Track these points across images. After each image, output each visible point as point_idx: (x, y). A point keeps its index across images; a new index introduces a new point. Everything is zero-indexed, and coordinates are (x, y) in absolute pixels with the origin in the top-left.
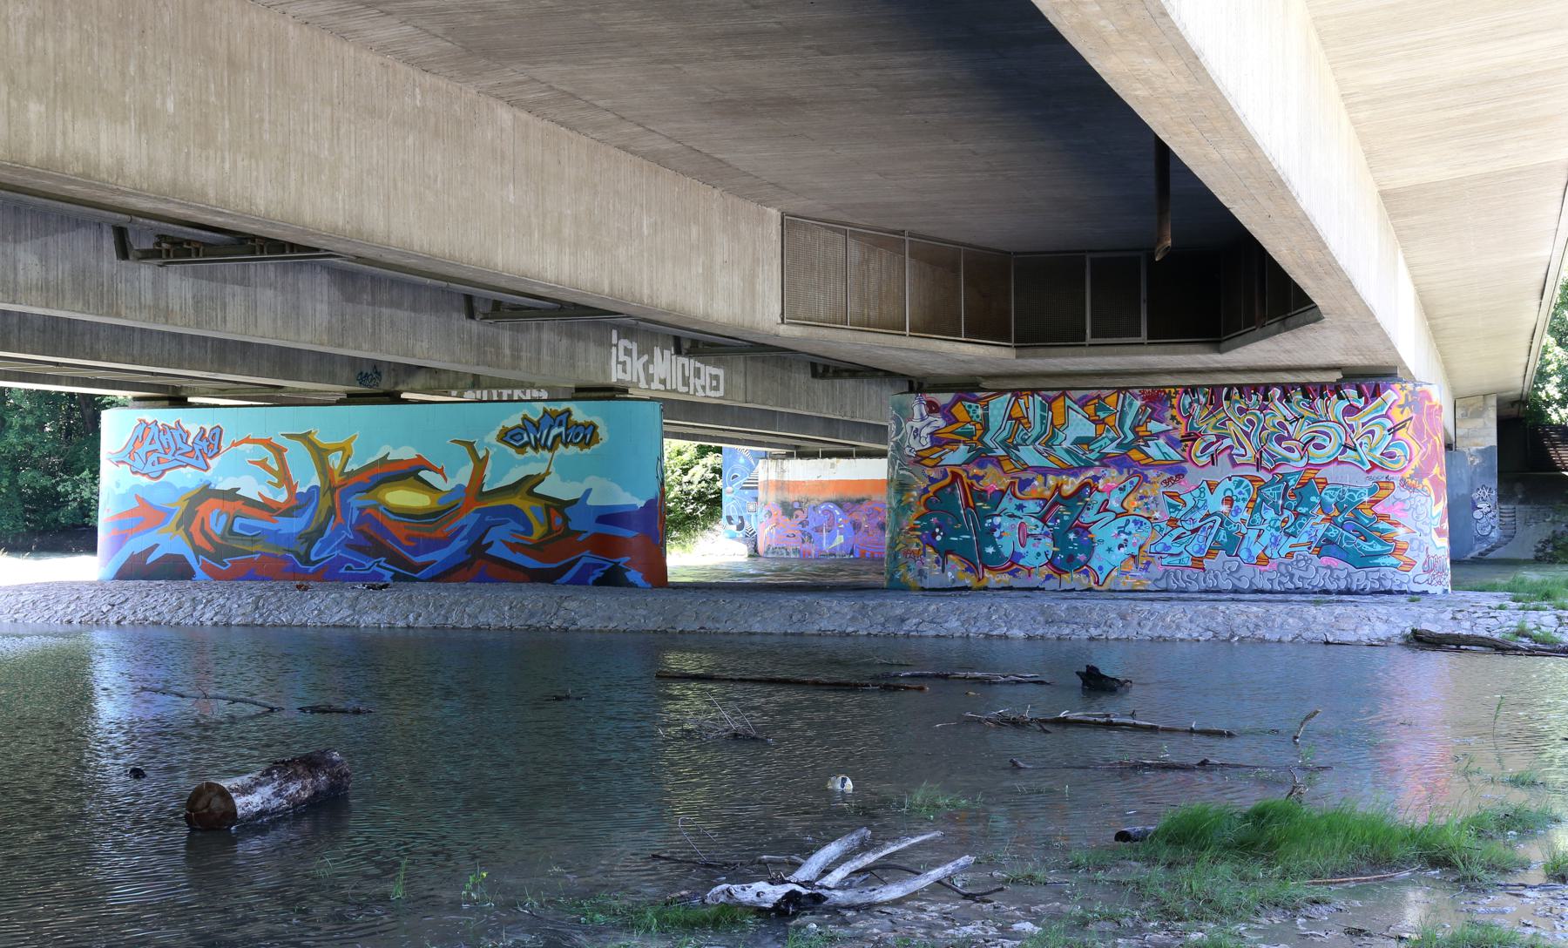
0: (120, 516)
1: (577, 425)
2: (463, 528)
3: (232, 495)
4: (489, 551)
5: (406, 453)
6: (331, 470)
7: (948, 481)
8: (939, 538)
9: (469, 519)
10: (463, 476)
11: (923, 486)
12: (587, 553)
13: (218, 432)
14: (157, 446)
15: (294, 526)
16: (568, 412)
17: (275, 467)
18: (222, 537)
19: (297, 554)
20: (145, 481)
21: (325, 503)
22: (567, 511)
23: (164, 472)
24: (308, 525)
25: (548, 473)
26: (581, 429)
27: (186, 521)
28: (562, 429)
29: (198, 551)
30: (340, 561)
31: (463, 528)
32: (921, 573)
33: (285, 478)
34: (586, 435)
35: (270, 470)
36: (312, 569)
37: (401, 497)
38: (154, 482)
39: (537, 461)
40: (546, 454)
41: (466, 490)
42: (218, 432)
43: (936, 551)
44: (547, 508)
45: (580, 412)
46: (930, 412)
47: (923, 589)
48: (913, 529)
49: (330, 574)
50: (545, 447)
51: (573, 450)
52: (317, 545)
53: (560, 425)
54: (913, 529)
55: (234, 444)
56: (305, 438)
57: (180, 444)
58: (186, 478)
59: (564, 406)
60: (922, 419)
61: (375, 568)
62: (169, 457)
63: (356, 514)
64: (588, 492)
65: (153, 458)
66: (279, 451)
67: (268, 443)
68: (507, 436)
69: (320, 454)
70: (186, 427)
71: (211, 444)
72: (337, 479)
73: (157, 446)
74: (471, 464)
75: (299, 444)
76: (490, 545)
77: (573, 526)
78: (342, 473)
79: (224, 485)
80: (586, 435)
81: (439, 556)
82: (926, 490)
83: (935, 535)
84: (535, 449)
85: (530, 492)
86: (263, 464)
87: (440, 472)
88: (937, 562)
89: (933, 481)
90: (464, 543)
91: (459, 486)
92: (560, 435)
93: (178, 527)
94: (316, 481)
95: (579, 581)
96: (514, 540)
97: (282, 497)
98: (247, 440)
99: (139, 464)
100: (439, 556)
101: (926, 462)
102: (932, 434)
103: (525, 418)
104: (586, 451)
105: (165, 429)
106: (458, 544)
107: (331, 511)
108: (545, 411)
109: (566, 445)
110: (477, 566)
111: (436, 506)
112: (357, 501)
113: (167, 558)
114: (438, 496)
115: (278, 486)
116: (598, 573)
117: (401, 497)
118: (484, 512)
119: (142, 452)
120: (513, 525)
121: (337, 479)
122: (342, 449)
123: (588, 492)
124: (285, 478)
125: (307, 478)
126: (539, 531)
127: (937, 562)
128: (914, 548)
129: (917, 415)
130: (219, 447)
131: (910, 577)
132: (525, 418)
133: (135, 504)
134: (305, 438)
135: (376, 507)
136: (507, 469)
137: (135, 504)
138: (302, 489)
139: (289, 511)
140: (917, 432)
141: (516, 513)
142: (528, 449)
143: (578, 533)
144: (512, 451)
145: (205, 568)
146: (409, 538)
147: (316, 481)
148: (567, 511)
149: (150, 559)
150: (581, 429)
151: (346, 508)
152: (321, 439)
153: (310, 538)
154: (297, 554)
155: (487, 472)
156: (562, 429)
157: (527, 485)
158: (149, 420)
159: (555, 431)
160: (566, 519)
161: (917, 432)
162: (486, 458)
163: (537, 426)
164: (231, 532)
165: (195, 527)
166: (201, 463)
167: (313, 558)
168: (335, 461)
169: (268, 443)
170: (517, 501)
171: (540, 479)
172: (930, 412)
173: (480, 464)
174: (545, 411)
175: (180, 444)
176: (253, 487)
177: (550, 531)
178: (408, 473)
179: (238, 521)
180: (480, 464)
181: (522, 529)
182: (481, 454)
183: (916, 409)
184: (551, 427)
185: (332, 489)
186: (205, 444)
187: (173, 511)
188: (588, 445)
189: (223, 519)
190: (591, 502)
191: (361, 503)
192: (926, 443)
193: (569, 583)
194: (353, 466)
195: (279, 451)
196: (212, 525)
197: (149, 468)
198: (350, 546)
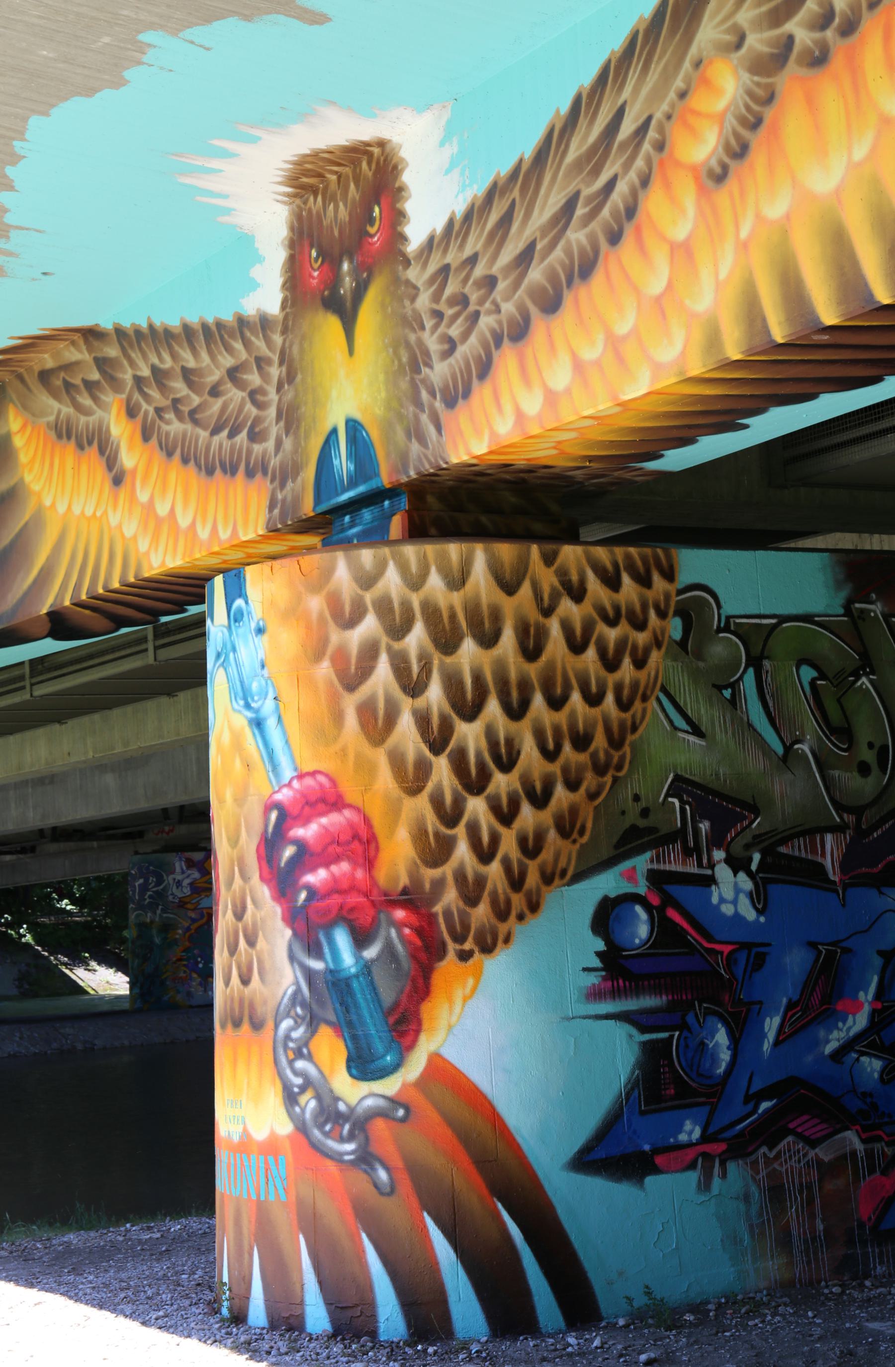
7: (205, 920)
8: (201, 966)
11: (186, 924)
32: (189, 994)
43: (199, 975)
46: (189, 867)
47: (191, 1007)
48: (180, 960)
54: (180, 960)
60: (183, 872)
82: (188, 929)
83: (197, 963)
88: (200, 984)
89: (194, 921)
101: (189, 906)
102: (191, 884)
127: (200, 984)
128: (182, 975)
129: (178, 869)
131: (179, 998)
140: (179, 884)
161: (179, 884)
172: (189, 867)
183: (177, 865)
192: (187, 891)
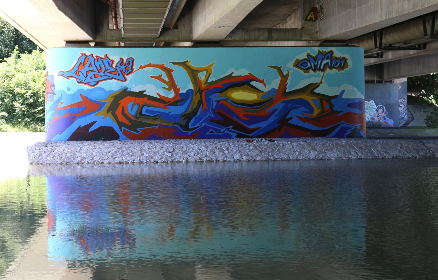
0: (71, 106)
1: (336, 59)
2: (275, 110)
3: (141, 94)
4: (290, 122)
5: (243, 72)
6: (200, 82)
9: (279, 106)
10: (275, 84)
12: (343, 122)
13: (131, 61)
14: (93, 68)
15: (178, 110)
16: (332, 52)
17: (167, 79)
18: (136, 117)
19: (181, 125)
20: (86, 87)
21: (197, 98)
22: (332, 101)
23: (98, 82)
24: (187, 110)
25: (321, 82)
26: (338, 61)
27: (113, 109)
28: (329, 61)
29: (121, 125)
30: (206, 129)
31: (275, 110)
33: (172, 85)
34: (342, 64)
35: (164, 81)
36: (190, 133)
37: (240, 95)
38: (91, 88)
39: (315, 76)
40: (321, 73)
41: (277, 91)
42: (131, 61)
44: (321, 100)
45: (338, 52)
49: (200, 135)
50: (319, 69)
51: (334, 71)
52: (193, 120)
53: (327, 58)
55: (141, 67)
56: (184, 64)
57: (108, 67)
58: (113, 86)
59: (329, 49)
61: (226, 132)
62: (101, 74)
63: (215, 104)
64: (343, 92)
65: (92, 74)
66: (169, 72)
67: (162, 67)
68: (299, 64)
69: (193, 73)
70: (111, 58)
71: (127, 67)
72: (203, 86)
73: (93, 68)
74: (279, 79)
75: (181, 68)
76: (291, 118)
77: (335, 109)
78: (206, 83)
79: (136, 89)
80: (342, 64)
81: (262, 125)
84: (314, 70)
85: (312, 93)
86: (159, 78)
87: (262, 82)
90: (277, 118)
91: (273, 89)
92: (328, 63)
93: (108, 111)
94: (191, 87)
95: (340, 135)
96: (303, 116)
97: (171, 95)
98: (149, 65)
99: (82, 78)
100: (262, 125)
103: (308, 55)
104: (341, 71)
105: (98, 59)
106: (272, 119)
107: (200, 103)
108: (319, 52)
109: (331, 68)
110: (283, 129)
111: (260, 99)
112: (215, 98)
113: (102, 129)
114: (262, 94)
115: (169, 89)
116: (349, 132)
117: (240, 95)
118: (287, 102)
119: (84, 71)
120: (303, 109)
121: (203, 86)
122: (206, 70)
123: (343, 92)
124: (172, 85)
125: (185, 85)
126: (317, 111)
130: (132, 69)
132: (308, 55)
133: (81, 100)
134: (184, 64)
135: (226, 100)
136: (299, 80)
137: (81, 100)
138: (183, 91)
139: (175, 102)
141: (306, 104)
142: (311, 70)
143: (340, 112)
144: (301, 71)
145: (125, 133)
146: (245, 116)
147: (191, 87)
148: (332, 101)
149: (91, 129)
150: (338, 61)
151: (209, 101)
152: (193, 64)
153: (188, 117)
154: (181, 125)
155: (288, 82)
156: (329, 61)
157: (310, 88)
158: (88, 54)
159: (325, 62)
160: (331, 105)
162: (288, 75)
163: (315, 59)
164: (141, 114)
165: (119, 112)
166: (121, 77)
167: (190, 127)
168: (202, 76)
169: (162, 67)
170: (305, 97)
171: (317, 85)
173: (284, 78)
174: (319, 52)
175: (108, 67)
176: (154, 89)
177: (323, 111)
178: (245, 83)
179: (145, 109)
180: (284, 78)
181: (307, 110)
182: (285, 73)
184: (322, 60)
185: (200, 91)
186: (123, 67)
187: (104, 104)
188: (342, 69)
189: (136, 108)
190: (344, 97)
191: (218, 99)
193: (333, 137)
194: (212, 79)
195: (169, 72)
196: (129, 110)
197: (88, 80)
198: (211, 120)
